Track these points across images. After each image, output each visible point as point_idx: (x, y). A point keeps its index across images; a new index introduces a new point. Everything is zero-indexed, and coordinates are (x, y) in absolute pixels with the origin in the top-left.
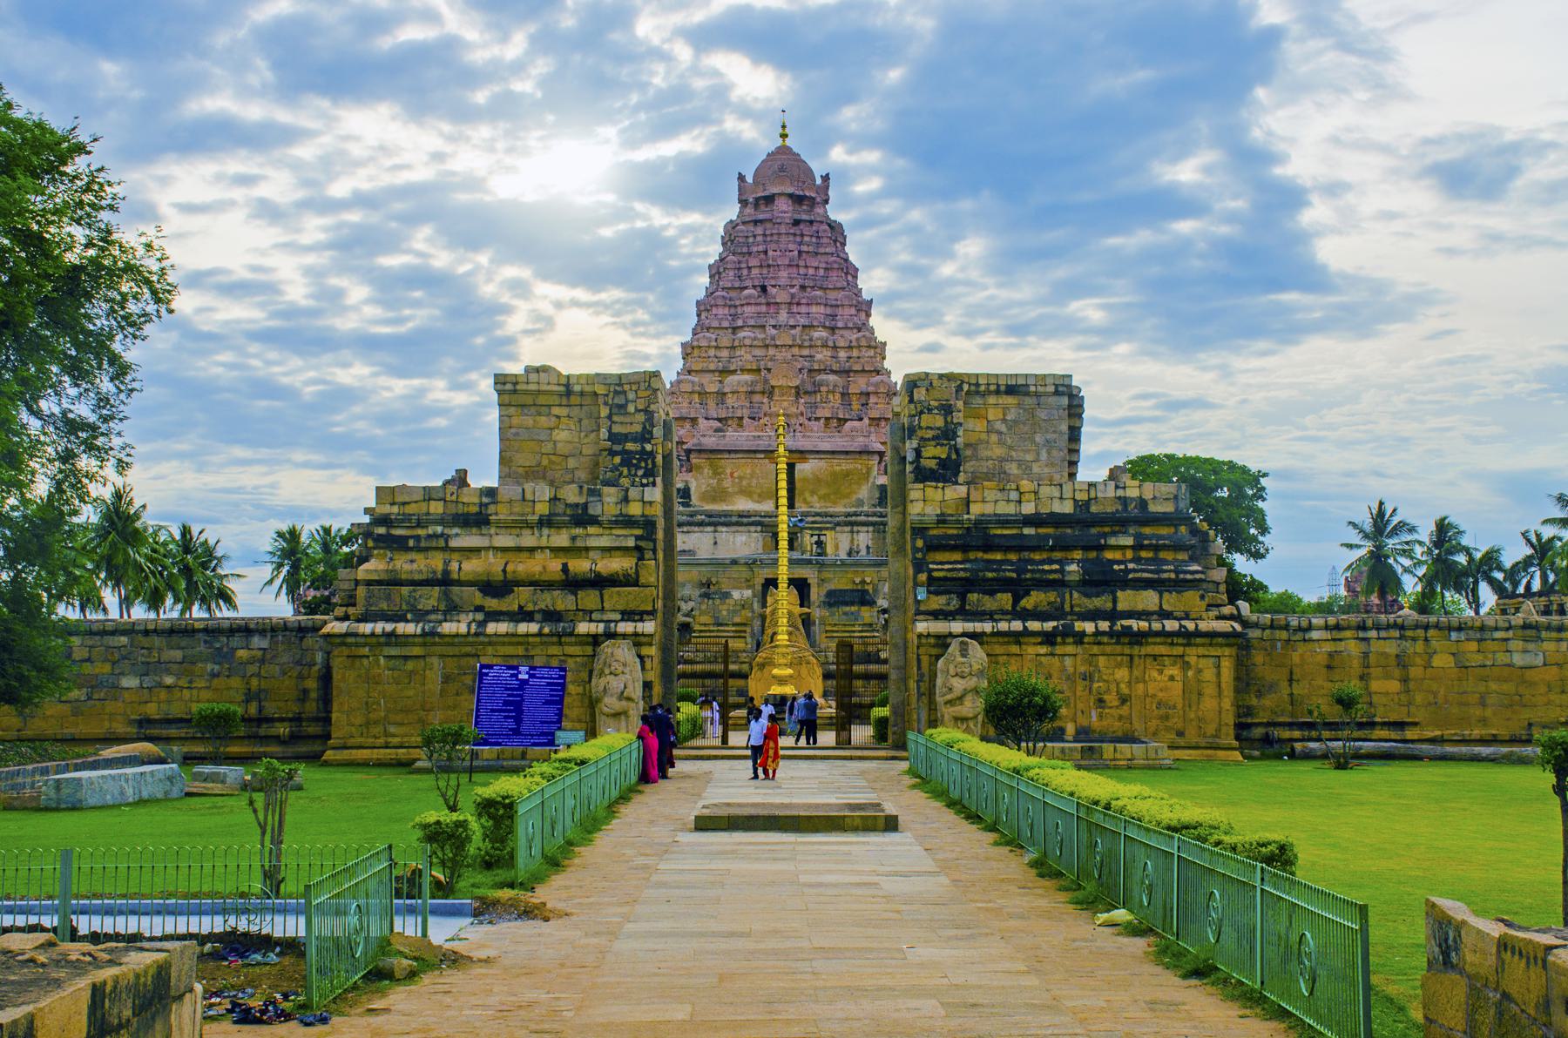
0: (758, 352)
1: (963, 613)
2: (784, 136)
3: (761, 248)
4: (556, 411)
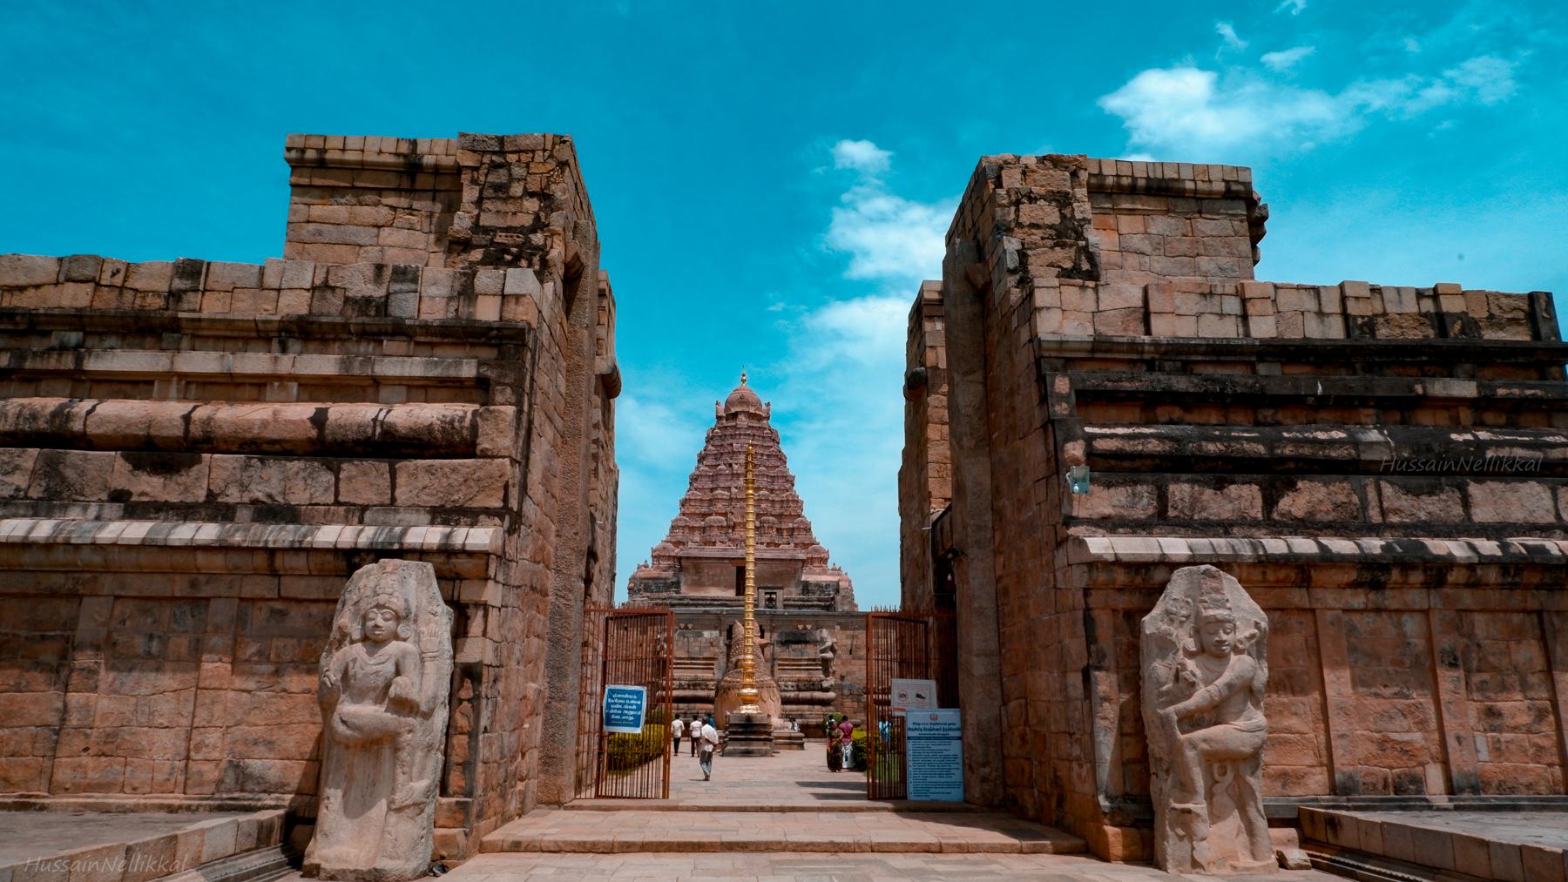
1: (1161, 520)
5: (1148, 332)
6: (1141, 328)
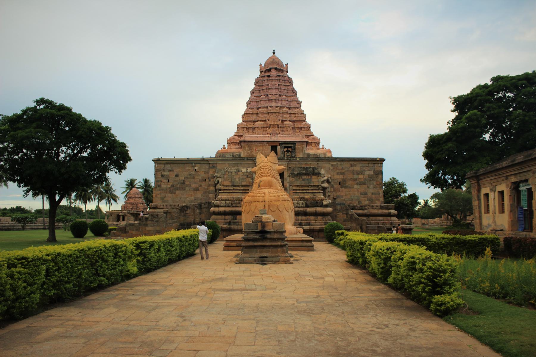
2: (274, 53)
3: (267, 84)
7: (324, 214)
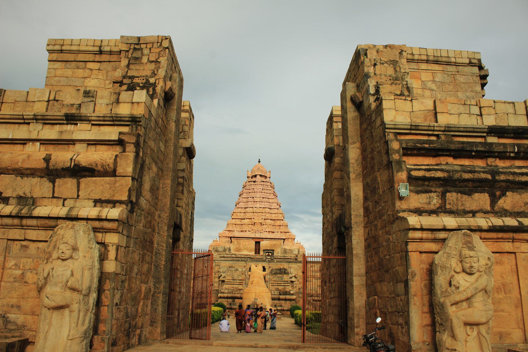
0: (252, 214)
2: (259, 162)
4: (90, 65)
5: (437, 122)
6: (433, 119)
7: (290, 300)
